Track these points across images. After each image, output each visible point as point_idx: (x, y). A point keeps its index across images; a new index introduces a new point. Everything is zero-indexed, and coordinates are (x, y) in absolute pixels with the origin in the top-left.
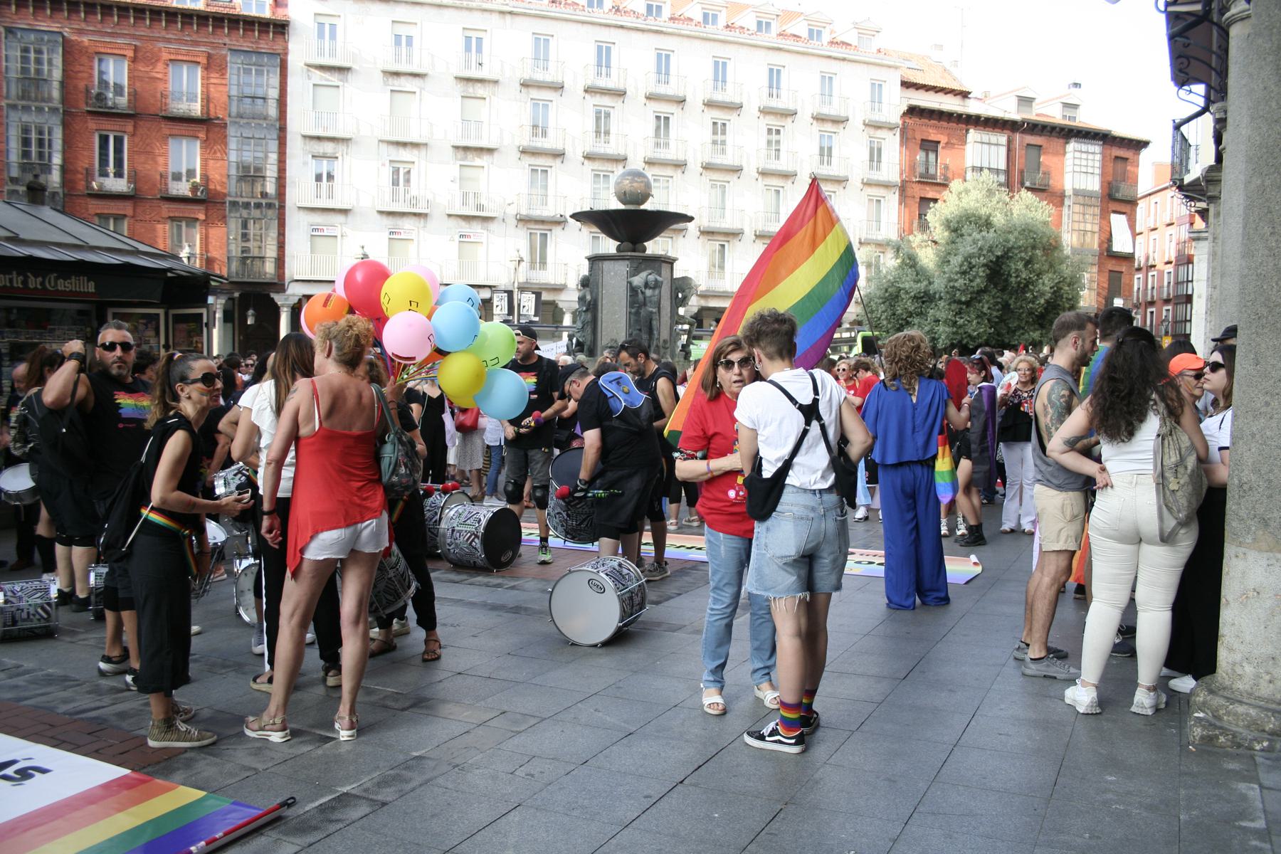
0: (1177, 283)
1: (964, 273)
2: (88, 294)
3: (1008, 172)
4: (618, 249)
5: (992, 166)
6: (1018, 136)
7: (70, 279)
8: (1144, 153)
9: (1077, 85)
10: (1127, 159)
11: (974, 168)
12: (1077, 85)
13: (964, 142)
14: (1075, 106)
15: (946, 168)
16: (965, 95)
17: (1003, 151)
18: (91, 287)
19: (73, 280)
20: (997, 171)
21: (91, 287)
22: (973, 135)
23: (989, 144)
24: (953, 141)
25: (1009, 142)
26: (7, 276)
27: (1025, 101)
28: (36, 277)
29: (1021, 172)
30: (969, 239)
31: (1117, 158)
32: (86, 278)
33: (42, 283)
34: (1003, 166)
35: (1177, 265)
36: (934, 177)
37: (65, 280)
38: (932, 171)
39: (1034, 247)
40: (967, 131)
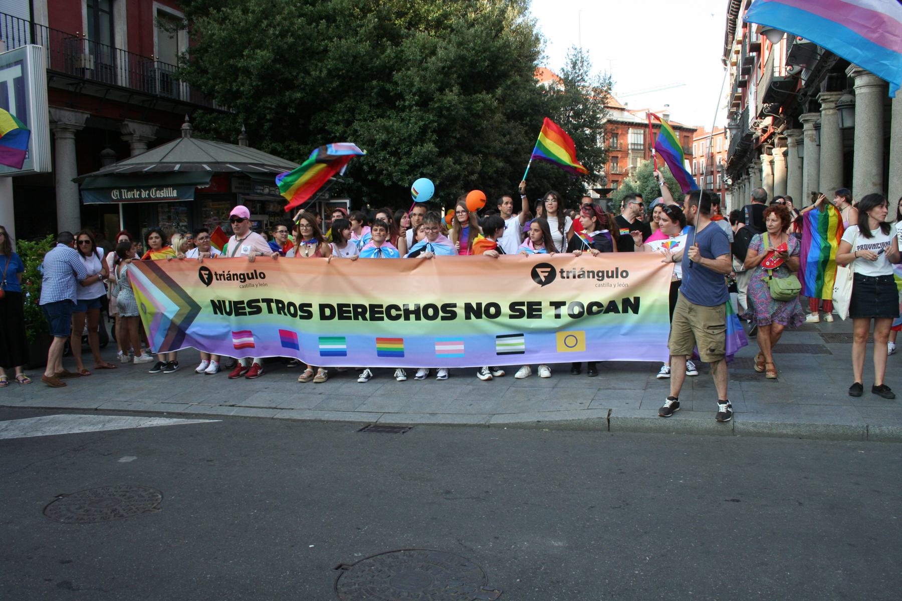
0: (707, 184)
1: (651, 193)
2: (174, 198)
3: (644, 145)
4: (601, 197)
5: (639, 143)
6: (647, 130)
7: (133, 191)
8: (695, 134)
9: (668, 106)
10: (688, 137)
11: (632, 144)
12: (668, 106)
13: (628, 133)
14: (668, 116)
15: (621, 144)
16: (623, 110)
17: (642, 136)
18: (175, 194)
19: (165, 190)
20: (640, 145)
21: (175, 194)
22: (631, 130)
23: (637, 134)
24: (624, 132)
25: (644, 132)
26: (132, 193)
27: (649, 115)
28: (145, 191)
29: (649, 144)
30: (652, 182)
31: (685, 136)
32: (126, 191)
33: (149, 195)
34: (642, 143)
35: (706, 176)
36: (617, 148)
37: (160, 191)
38: (615, 146)
39: (672, 184)
40: (629, 128)
